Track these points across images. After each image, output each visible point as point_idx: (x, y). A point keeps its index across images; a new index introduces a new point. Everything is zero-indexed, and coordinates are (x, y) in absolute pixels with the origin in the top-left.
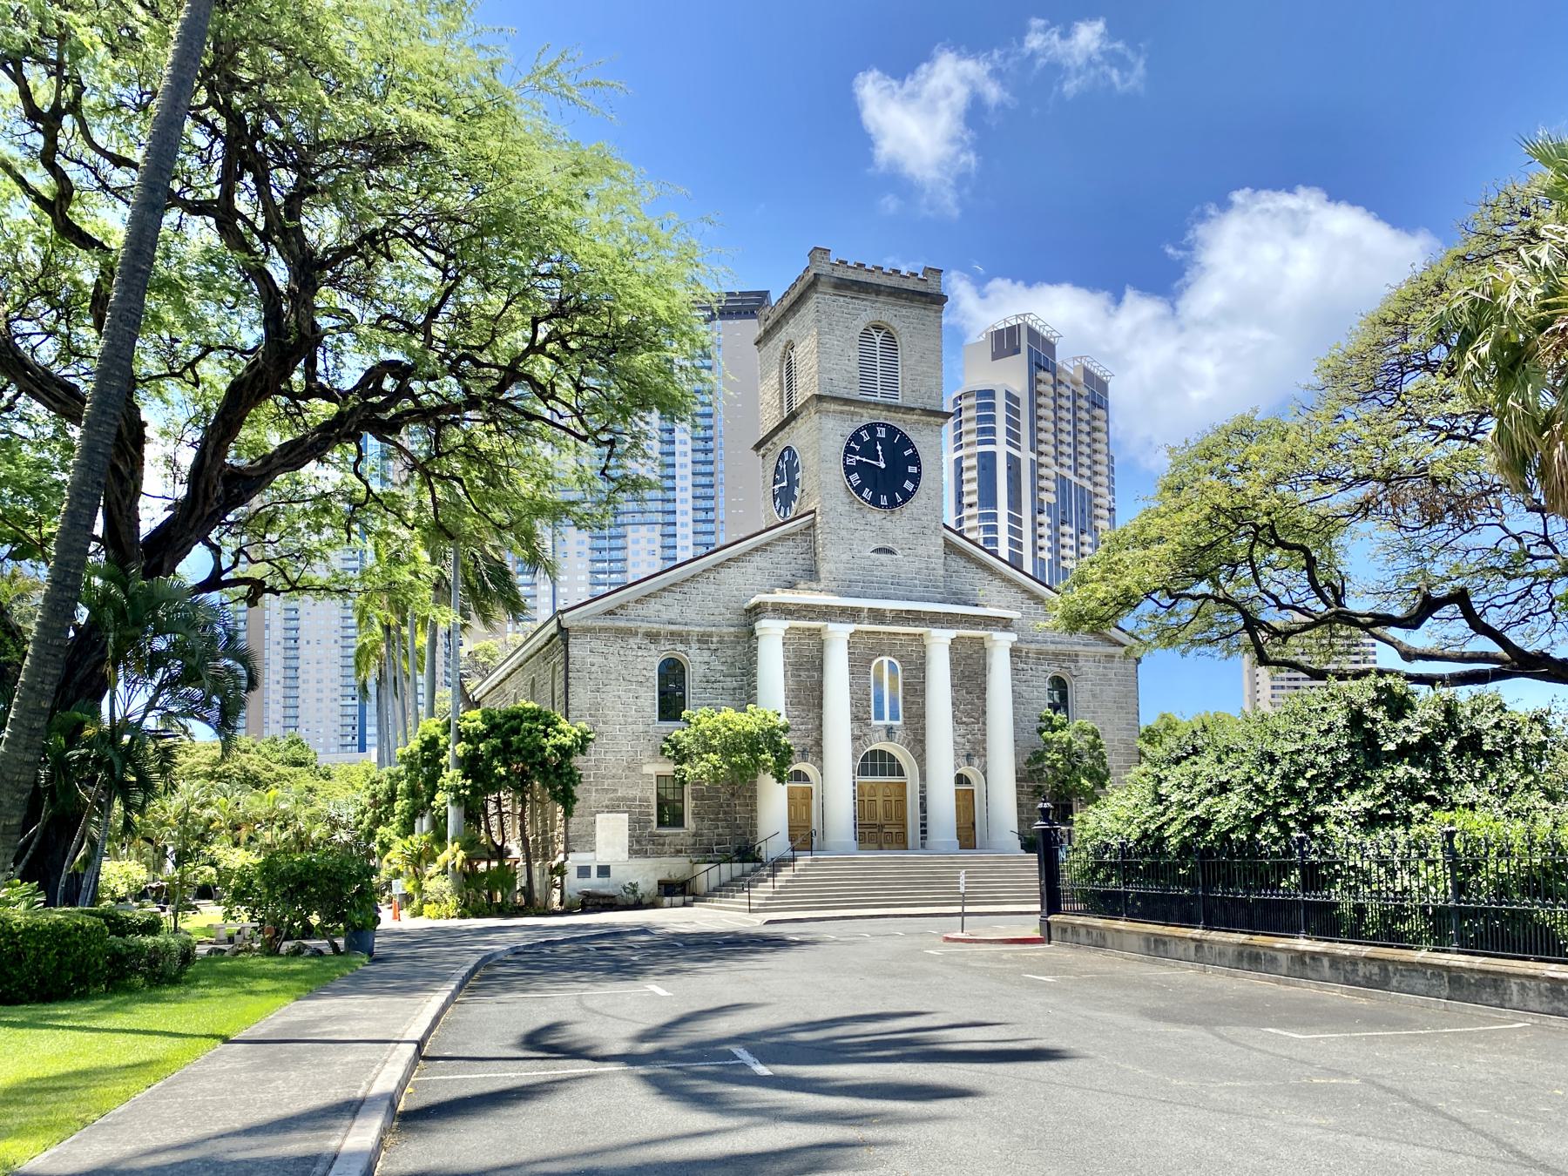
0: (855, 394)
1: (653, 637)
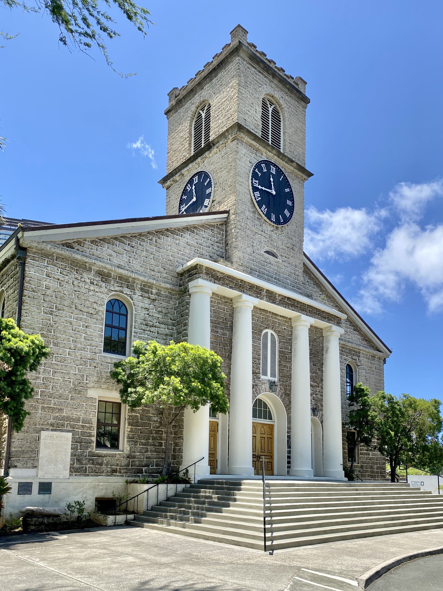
1: (104, 276)
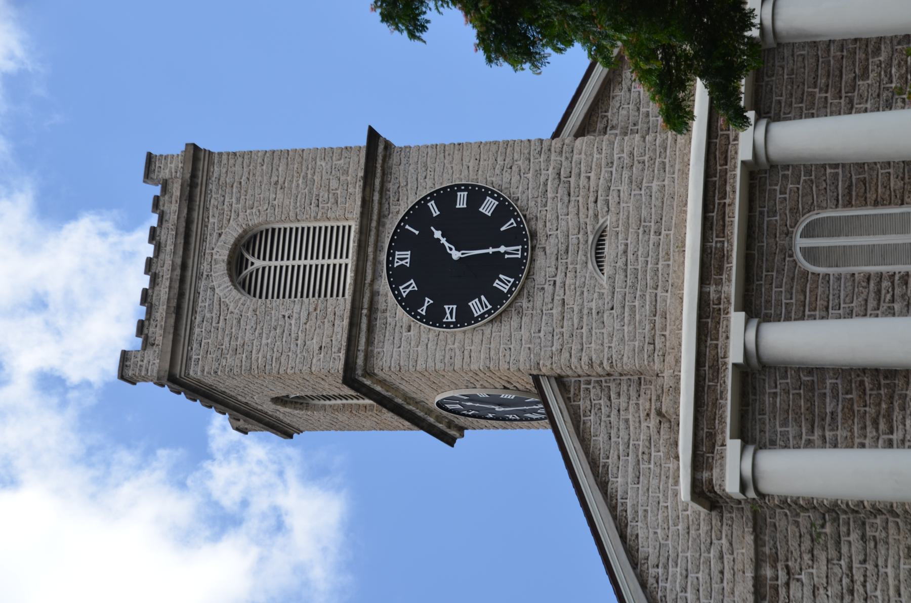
0: (344, 304)
